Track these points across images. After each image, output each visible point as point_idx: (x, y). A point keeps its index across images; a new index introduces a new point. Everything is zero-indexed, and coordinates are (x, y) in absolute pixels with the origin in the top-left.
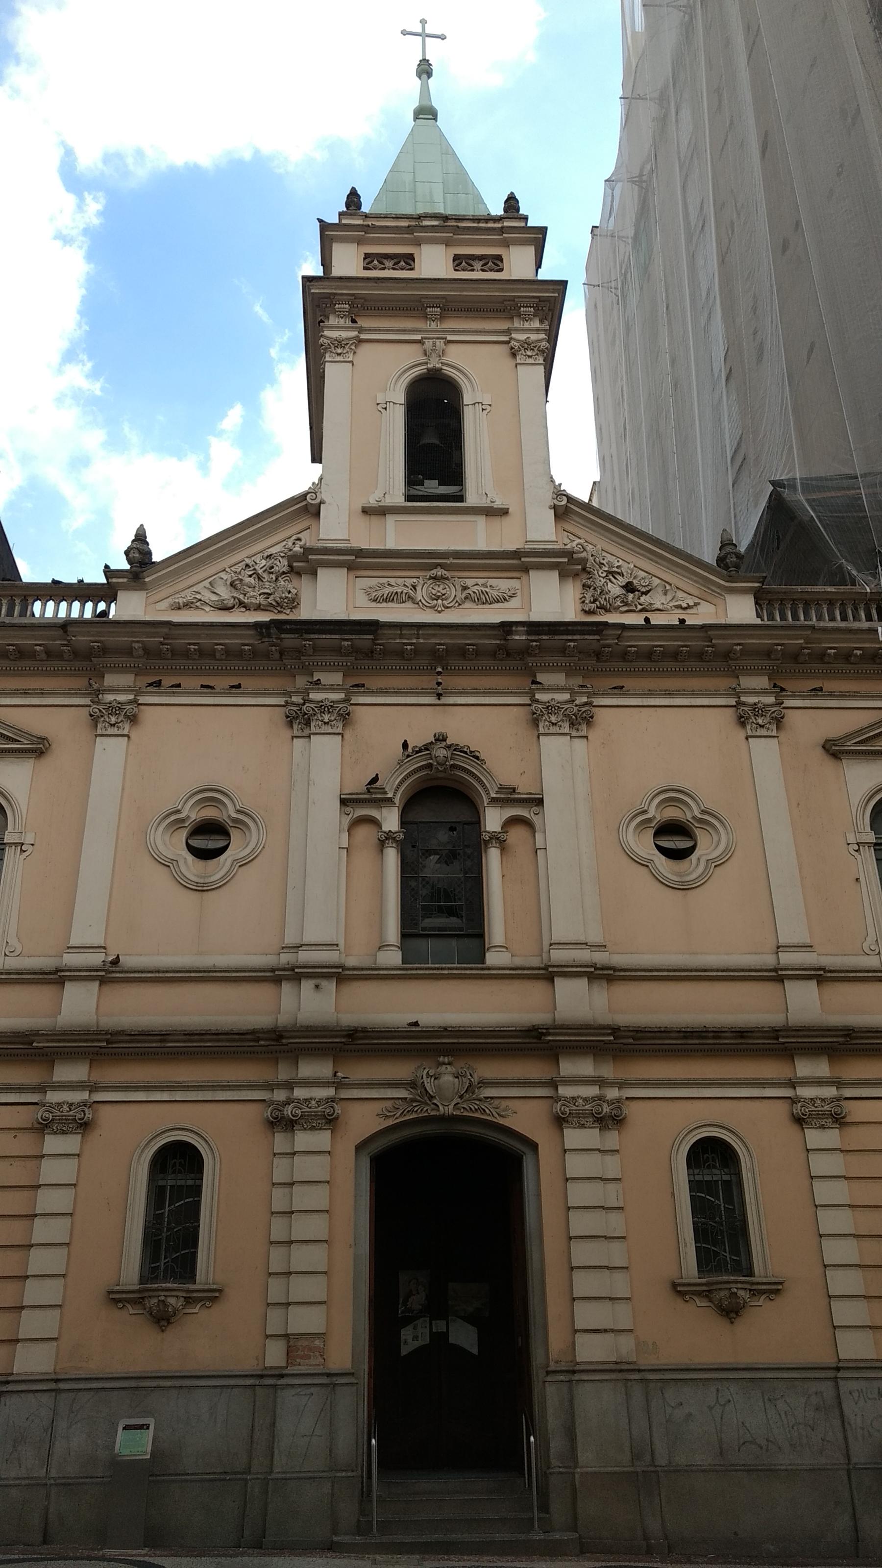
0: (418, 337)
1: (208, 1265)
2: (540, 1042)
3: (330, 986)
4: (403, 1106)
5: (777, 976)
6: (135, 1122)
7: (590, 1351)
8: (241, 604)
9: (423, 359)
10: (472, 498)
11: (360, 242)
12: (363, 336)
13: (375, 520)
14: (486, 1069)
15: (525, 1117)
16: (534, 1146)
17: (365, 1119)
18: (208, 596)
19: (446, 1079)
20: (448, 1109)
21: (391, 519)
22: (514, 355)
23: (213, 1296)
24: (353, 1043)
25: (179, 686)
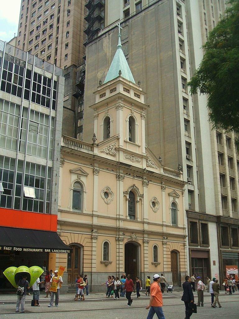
0: (131, 109)
1: (111, 259)
2: (143, 232)
3: (123, 221)
4: (129, 239)
5: (163, 225)
6: (102, 239)
7: (146, 270)
8: (109, 154)
9: (131, 114)
10: (136, 143)
11: (123, 85)
12: (125, 106)
13: (125, 143)
14: (137, 235)
15: (140, 242)
16: (140, 245)
17: (126, 241)
18: (105, 151)
19: (133, 236)
20: (133, 240)
21: (127, 144)
22: (141, 117)
23: (111, 263)
24: (125, 231)
25: (108, 169)
